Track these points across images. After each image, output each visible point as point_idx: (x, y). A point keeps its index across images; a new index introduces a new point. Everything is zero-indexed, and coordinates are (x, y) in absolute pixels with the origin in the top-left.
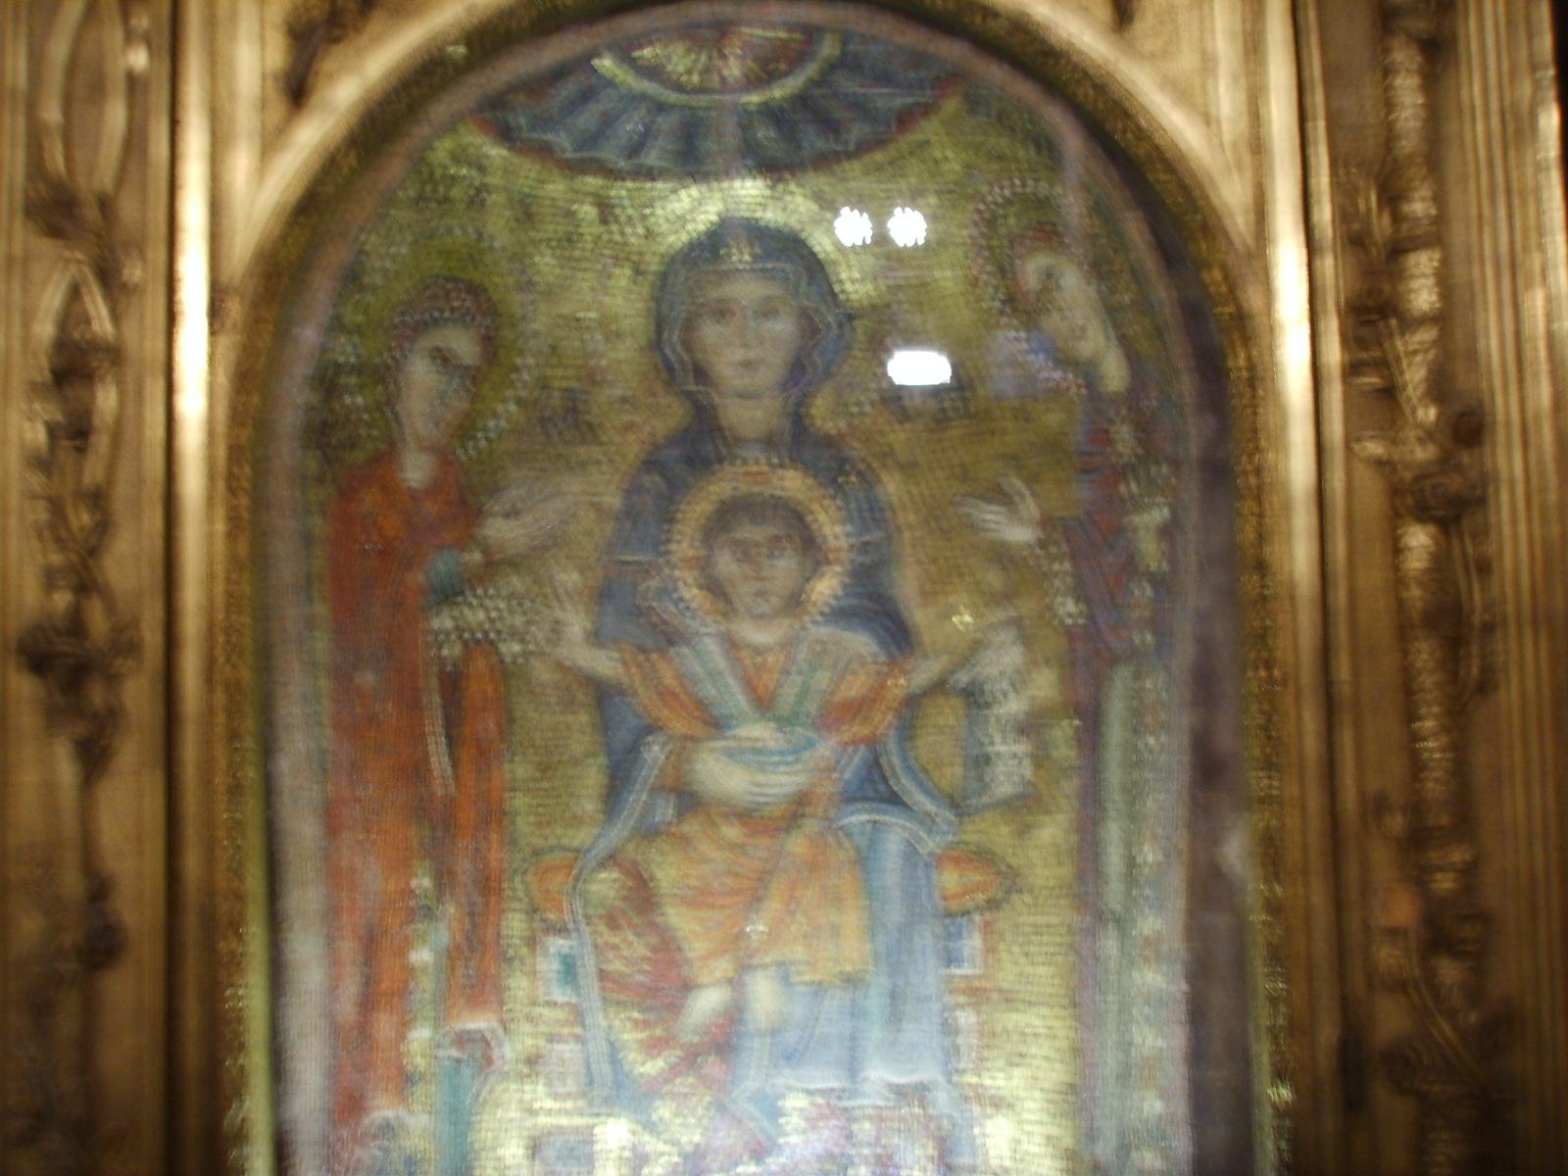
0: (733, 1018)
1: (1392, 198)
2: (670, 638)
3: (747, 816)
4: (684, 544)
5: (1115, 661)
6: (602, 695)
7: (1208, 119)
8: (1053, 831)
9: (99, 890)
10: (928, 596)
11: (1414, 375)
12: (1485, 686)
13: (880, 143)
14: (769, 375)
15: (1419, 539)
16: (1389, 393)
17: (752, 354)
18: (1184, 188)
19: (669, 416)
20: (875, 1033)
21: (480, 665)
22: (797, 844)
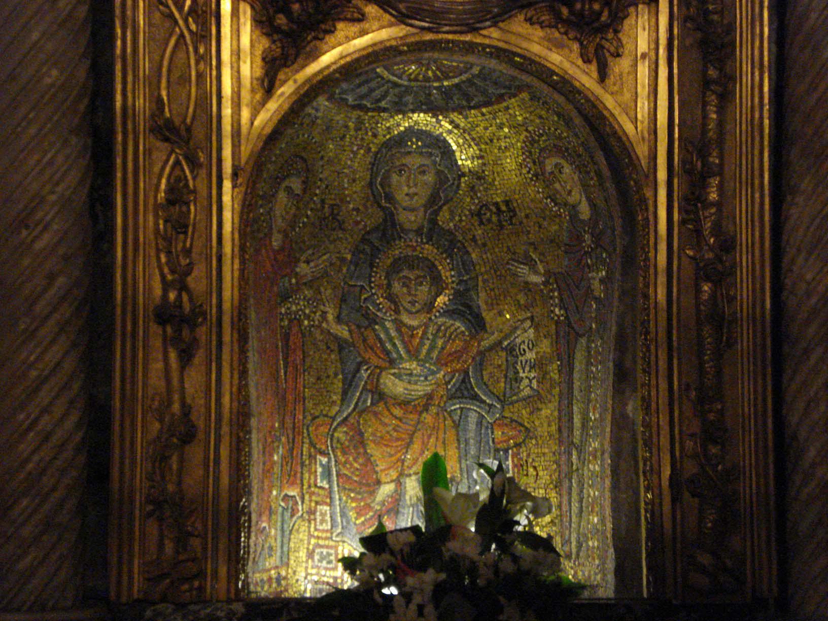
1: (703, 154)
3: (404, 404)
4: (380, 277)
5: (578, 335)
6: (342, 346)
7: (635, 121)
8: (548, 411)
9: (186, 410)
10: (491, 306)
12: (730, 344)
13: (487, 104)
16: (698, 232)
17: (413, 190)
19: (374, 218)
21: (295, 329)
22: (428, 418)
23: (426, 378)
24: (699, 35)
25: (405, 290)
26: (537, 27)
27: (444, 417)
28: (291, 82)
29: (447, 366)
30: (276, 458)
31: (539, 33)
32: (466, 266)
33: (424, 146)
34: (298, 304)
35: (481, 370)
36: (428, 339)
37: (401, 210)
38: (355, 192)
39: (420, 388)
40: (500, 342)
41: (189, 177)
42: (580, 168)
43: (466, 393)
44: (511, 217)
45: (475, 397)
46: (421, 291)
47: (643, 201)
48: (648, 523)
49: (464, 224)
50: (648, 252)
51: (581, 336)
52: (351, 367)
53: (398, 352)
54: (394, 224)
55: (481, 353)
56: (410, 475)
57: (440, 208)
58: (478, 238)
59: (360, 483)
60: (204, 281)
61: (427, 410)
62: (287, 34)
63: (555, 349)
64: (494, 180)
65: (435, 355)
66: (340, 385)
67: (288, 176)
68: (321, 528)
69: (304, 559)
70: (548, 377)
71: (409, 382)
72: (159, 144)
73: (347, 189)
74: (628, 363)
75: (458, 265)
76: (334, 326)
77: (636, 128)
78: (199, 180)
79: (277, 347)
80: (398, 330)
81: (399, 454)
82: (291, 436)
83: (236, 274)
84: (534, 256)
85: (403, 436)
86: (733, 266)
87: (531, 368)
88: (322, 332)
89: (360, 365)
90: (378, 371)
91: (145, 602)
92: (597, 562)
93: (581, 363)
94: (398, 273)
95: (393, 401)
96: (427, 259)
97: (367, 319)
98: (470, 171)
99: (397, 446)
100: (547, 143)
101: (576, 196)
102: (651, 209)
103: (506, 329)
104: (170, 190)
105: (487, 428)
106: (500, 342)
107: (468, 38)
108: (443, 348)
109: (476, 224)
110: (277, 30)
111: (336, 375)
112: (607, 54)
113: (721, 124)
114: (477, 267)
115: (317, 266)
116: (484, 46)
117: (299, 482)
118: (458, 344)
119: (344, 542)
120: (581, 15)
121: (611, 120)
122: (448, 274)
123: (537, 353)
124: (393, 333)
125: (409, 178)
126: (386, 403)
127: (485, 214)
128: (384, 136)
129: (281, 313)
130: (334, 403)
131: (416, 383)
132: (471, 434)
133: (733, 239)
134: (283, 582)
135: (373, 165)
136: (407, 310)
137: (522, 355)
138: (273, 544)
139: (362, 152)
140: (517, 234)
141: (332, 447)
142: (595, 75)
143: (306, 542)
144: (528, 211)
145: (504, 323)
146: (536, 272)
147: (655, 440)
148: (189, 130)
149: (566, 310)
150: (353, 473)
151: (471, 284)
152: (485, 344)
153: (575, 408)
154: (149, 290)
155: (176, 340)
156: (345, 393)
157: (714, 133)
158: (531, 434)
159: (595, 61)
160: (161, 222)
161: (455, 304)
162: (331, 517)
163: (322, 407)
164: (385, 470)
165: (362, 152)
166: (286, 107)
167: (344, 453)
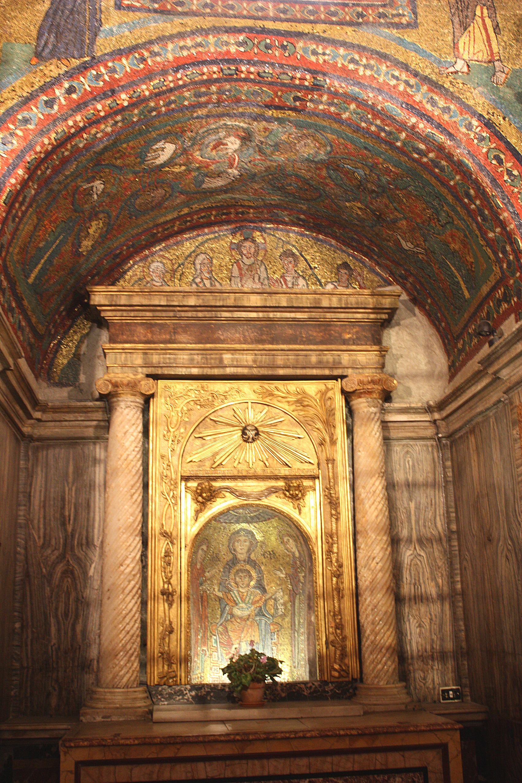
1: (332, 538)
2: (230, 591)
3: (241, 618)
4: (232, 576)
6: (220, 599)
8: (287, 619)
9: (171, 623)
10: (268, 585)
11: (334, 560)
14: (244, 551)
15: (334, 579)
18: (308, 536)
22: (248, 622)
31: (279, 500)
32: (260, 572)
42: (295, 541)
45: (264, 615)
47: (314, 552)
52: (223, 606)
62: (203, 503)
65: (250, 601)
72: (162, 538)
74: (312, 604)
91: (159, 685)
101: (294, 549)
104: (166, 552)
110: (198, 502)
113: (337, 528)
118: (258, 598)
120: (292, 495)
124: (237, 595)
152: (267, 597)
154: (158, 584)
155: (168, 600)
166: (201, 525)
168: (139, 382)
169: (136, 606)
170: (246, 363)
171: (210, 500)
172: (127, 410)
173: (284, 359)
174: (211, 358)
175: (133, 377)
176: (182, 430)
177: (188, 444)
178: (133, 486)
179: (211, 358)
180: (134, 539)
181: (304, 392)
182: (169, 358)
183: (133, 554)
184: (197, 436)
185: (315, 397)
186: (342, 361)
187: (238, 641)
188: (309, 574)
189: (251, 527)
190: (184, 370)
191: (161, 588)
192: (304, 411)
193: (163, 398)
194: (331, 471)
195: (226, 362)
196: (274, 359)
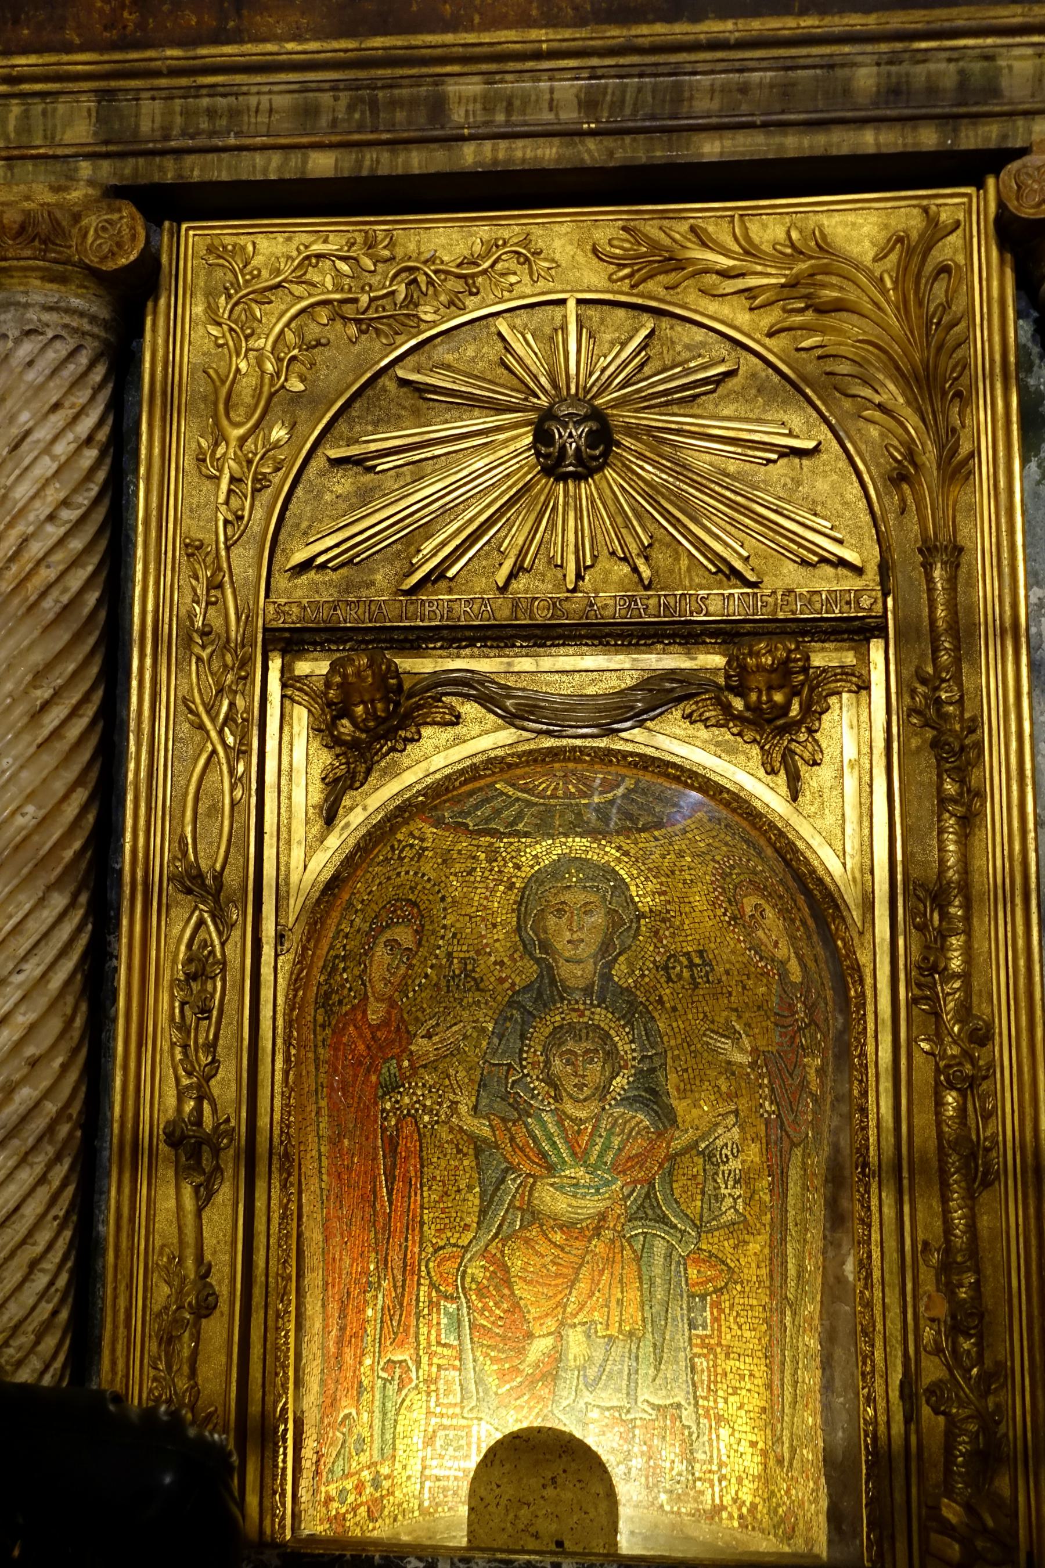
0: (557, 1356)
1: (942, 906)
3: (567, 1226)
4: (535, 1052)
5: (794, 1145)
6: (480, 1147)
8: (756, 1246)
9: (204, 1271)
10: (683, 1094)
14: (586, 950)
17: (575, 936)
20: (647, 1370)
22: (598, 1246)
23: (597, 1190)
24: (930, 734)
25: (569, 1069)
26: (699, 725)
27: (623, 1248)
28: (359, 809)
29: (625, 1174)
30: (370, 1312)
31: (703, 733)
32: (651, 1037)
33: (587, 878)
34: (414, 1093)
35: (671, 1183)
36: (601, 1136)
37: (562, 961)
38: (498, 940)
39: (590, 1204)
40: (696, 1143)
41: (216, 942)
42: (783, 913)
43: (650, 1212)
44: (707, 974)
45: (663, 1220)
46: (592, 1071)
47: (857, 968)
48: (868, 1453)
49: (647, 980)
50: (865, 1044)
51: (797, 1145)
52: (492, 1175)
53: (559, 1154)
54: (553, 982)
55: (672, 1158)
56: (574, 1326)
57: (615, 959)
58: (665, 998)
59: (504, 1338)
60: (233, 1085)
61: (599, 1235)
63: (764, 1159)
64: (683, 923)
65: (609, 1158)
66: (477, 1202)
67: (388, 926)
68: (446, 1401)
69: (421, 1446)
70: (757, 1197)
71: (574, 1196)
72: (180, 897)
73: (484, 937)
74: (845, 1204)
75: (640, 1035)
76: (470, 1119)
77: (844, 865)
78: (229, 946)
79: (374, 1159)
80: (560, 1123)
81: (560, 1296)
82: (400, 1277)
83: (279, 1076)
84: (737, 1027)
85: (565, 1271)
86: (991, 1065)
87: (736, 1182)
88: (451, 1130)
89: (506, 1171)
90: (531, 1180)
92: (811, 1484)
93: (796, 1184)
94: (560, 1045)
95: (552, 1223)
96: (598, 1027)
97: (516, 1109)
98: (651, 911)
99: (556, 1285)
100: (742, 877)
101: (783, 951)
102: (869, 981)
103: (704, 1127)
104: (189, 961)
105: (678, 1263)
106: (696, 1143)
107: (603, 743)
108: (620, 1150)
109: (663, 980)
111: (470, 1187)
112: (800, 763)
113: (965, 860)
114: (665, 1039)
115: (441, 1042)
116: (625, 755)
117: (412, 1339)
118: (634, 1148)
119: (480, 1419)
121: (808, 854)
122: (627, 1047)
123: (743, 1162)
124: (553, 1129)
125: (570, 921)
126: (541, 1225)
127: (674, 968)
128: (532, 867)
129: (383, 1110)
130: (467, 1227)
131: (584, 1196)
132: (658, 1271)
133: (989, 1026)
134: (386, 1484)
135: (520, 904)
136: (571, 1096)
137: (724, 1163)
138: (365, 1433)
139: (502, 888)
140: (715, 996)
141: (463, 1288)
142: (784, 790)
143: (423, 1422)
144: (728, 966)
145: (700, 1117)
146: (742, 1050)
147: (879, 1326)
148: (218, 877)
149: (778, 1105)
150: (493, 1323)
151: (657, 1062)
152: (677, 1145)
153: (790, 1250)
156: (483, 1212)
157: (955, 872)
158: (735, 1277)
159: (782, 772)
160: (177, 1004)
161: (637, 1089)
162: (461, 1385)
163: (449, 1234)
164: (540, 1318)
165: (502, 888)
167: (481, 1296)
168: (76, 218)
169: (43, 1194)
170: (548, 116)
171: (390, 734)
172: (27, 349)
173: (725, 89)
174: (394, 104)
175: (50, 198)
176: (279, 433)
177: (299, 491)
178: (39, 676)
179: (394, 104)
180: (41, 902)
181: (824, 246)
182: (211, 113)
183: (33, 969)
184: (334, 454)
185: (878, 269)
186: (1004, 83)
187: (551, 1324)
188: (838, 1069)
189: (607, 853)
190: (276, 159)
191: (171, 1114)
192: (823, 331)
193: (200, 298)
194: (941, 598)
195: (458, 115)
196: (678, 87)
